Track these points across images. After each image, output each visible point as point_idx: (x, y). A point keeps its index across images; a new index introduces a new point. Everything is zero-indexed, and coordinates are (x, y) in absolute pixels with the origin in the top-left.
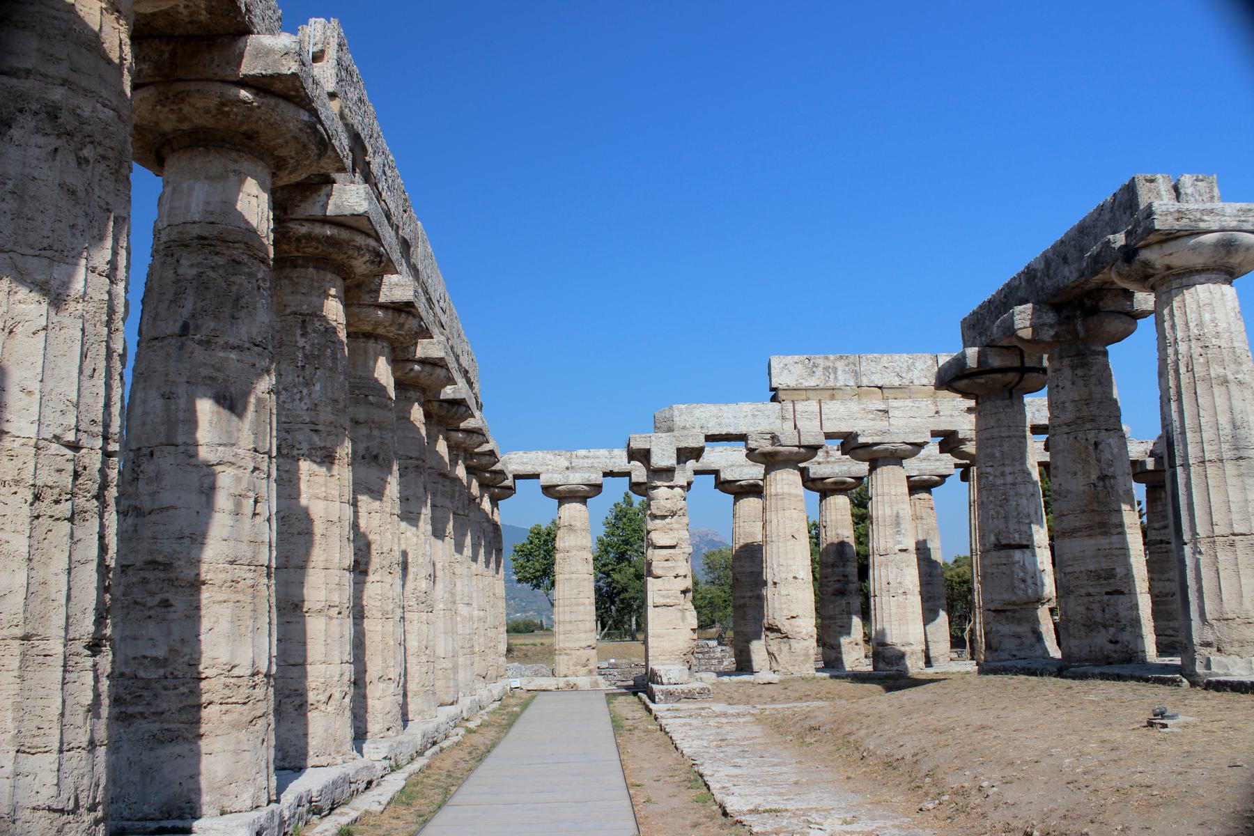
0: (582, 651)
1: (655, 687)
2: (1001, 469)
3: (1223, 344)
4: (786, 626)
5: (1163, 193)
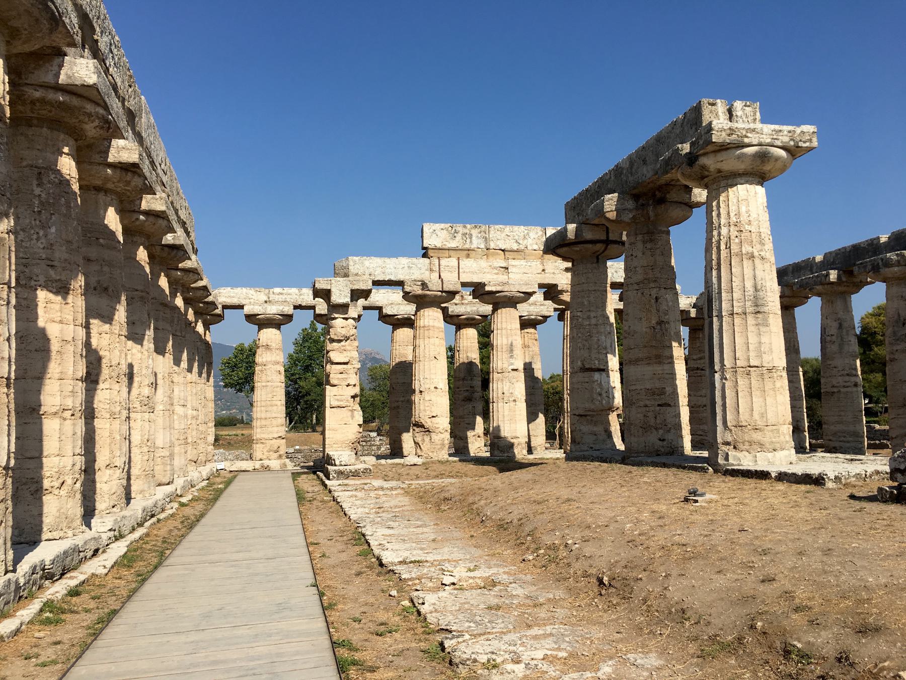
0: (274, 440)
1: (329, 467)
2: (588, 313)
4: (428, 423)
5: (720, 114)
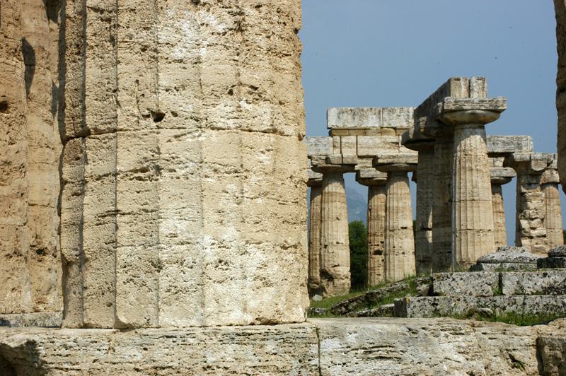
2: (426, 190)
3: (473, 153)
